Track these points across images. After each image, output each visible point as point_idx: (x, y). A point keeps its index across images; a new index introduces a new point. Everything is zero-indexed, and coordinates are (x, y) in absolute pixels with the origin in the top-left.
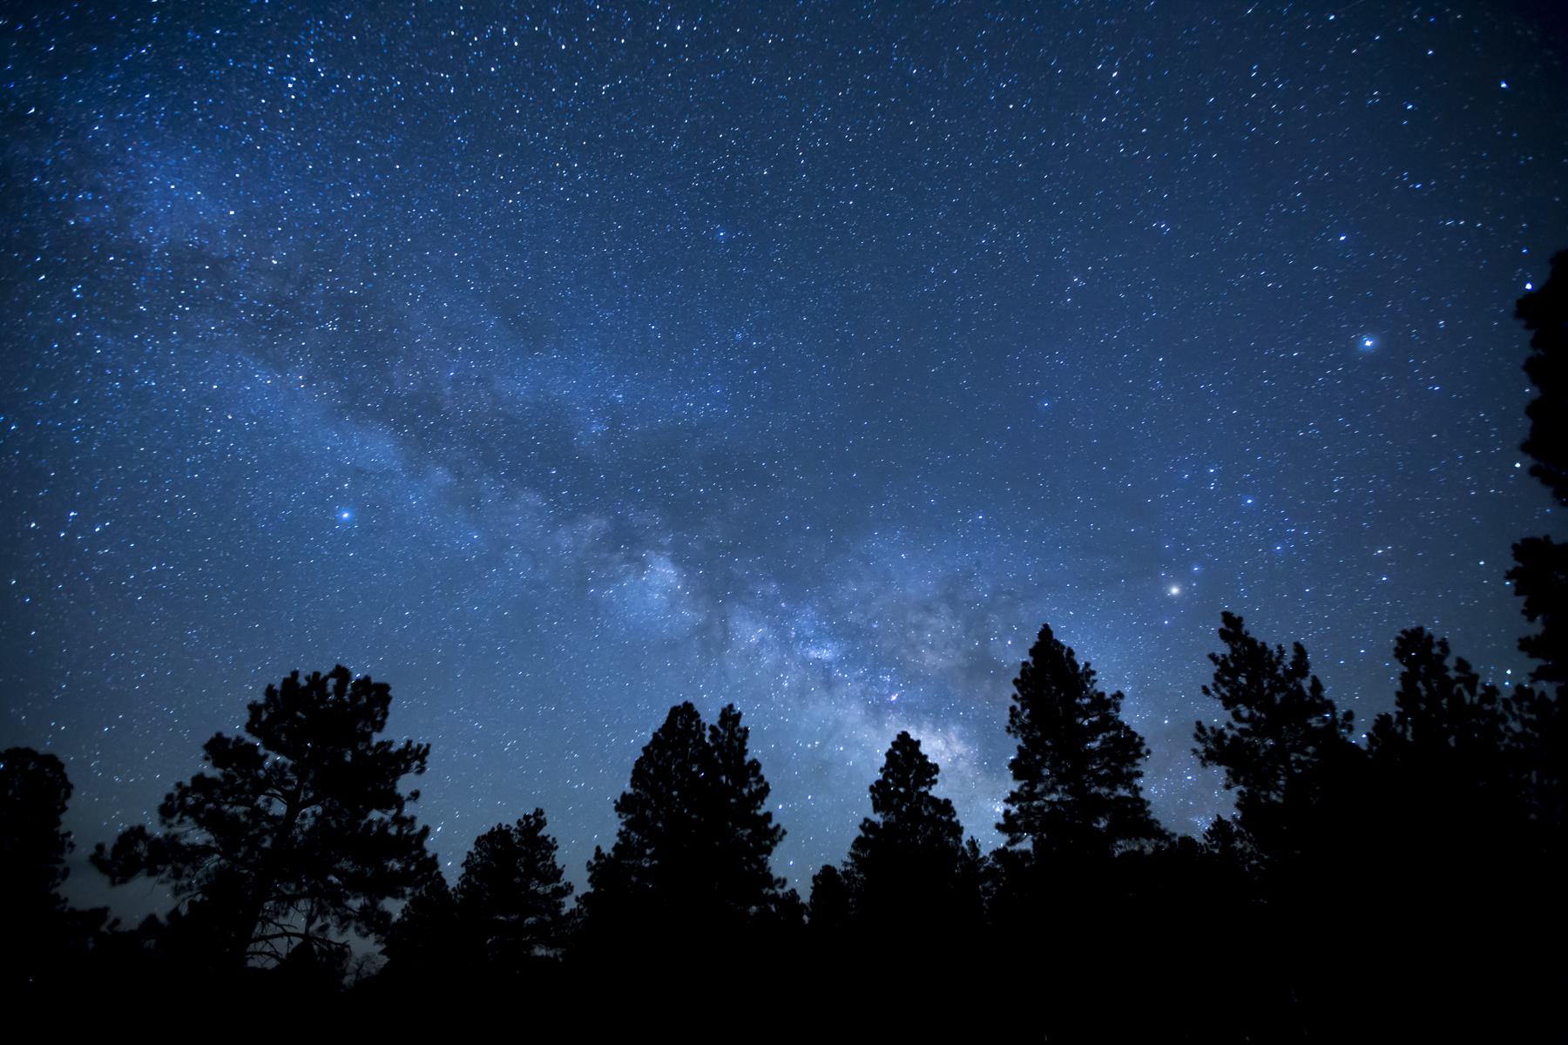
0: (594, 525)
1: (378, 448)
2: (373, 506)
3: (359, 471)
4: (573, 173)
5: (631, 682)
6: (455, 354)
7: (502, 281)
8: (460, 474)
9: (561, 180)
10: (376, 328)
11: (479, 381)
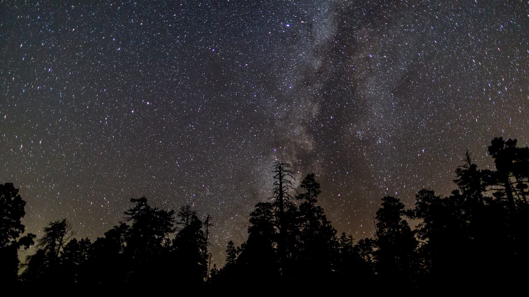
0: (309, 144)
1: (325, 31)
2: (295, 36)
3: (311, 26)
4: (501, 88)
5: (233, 179)
6: (381, 54)
7: (428, 68)
8: (319, 72)
9: (495, 83)
10: (386, 14)
11: (371, 70)
